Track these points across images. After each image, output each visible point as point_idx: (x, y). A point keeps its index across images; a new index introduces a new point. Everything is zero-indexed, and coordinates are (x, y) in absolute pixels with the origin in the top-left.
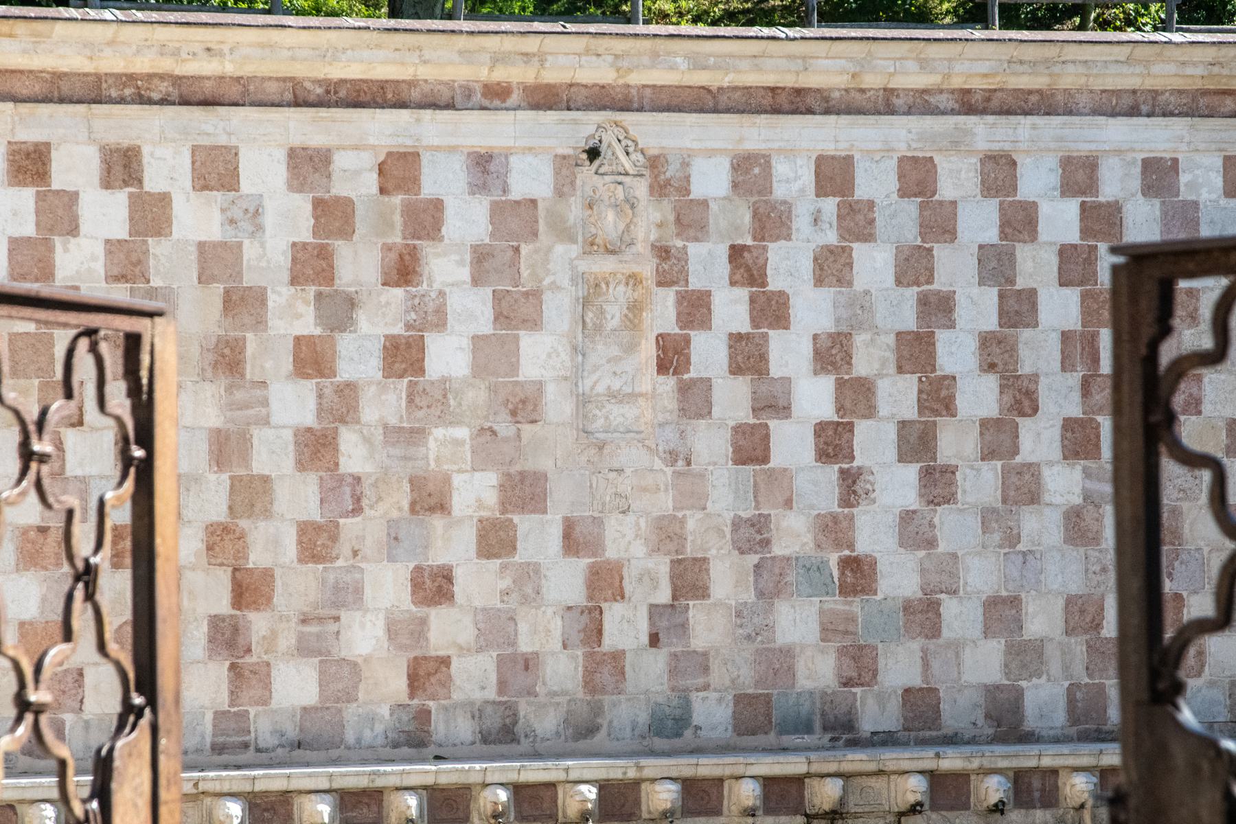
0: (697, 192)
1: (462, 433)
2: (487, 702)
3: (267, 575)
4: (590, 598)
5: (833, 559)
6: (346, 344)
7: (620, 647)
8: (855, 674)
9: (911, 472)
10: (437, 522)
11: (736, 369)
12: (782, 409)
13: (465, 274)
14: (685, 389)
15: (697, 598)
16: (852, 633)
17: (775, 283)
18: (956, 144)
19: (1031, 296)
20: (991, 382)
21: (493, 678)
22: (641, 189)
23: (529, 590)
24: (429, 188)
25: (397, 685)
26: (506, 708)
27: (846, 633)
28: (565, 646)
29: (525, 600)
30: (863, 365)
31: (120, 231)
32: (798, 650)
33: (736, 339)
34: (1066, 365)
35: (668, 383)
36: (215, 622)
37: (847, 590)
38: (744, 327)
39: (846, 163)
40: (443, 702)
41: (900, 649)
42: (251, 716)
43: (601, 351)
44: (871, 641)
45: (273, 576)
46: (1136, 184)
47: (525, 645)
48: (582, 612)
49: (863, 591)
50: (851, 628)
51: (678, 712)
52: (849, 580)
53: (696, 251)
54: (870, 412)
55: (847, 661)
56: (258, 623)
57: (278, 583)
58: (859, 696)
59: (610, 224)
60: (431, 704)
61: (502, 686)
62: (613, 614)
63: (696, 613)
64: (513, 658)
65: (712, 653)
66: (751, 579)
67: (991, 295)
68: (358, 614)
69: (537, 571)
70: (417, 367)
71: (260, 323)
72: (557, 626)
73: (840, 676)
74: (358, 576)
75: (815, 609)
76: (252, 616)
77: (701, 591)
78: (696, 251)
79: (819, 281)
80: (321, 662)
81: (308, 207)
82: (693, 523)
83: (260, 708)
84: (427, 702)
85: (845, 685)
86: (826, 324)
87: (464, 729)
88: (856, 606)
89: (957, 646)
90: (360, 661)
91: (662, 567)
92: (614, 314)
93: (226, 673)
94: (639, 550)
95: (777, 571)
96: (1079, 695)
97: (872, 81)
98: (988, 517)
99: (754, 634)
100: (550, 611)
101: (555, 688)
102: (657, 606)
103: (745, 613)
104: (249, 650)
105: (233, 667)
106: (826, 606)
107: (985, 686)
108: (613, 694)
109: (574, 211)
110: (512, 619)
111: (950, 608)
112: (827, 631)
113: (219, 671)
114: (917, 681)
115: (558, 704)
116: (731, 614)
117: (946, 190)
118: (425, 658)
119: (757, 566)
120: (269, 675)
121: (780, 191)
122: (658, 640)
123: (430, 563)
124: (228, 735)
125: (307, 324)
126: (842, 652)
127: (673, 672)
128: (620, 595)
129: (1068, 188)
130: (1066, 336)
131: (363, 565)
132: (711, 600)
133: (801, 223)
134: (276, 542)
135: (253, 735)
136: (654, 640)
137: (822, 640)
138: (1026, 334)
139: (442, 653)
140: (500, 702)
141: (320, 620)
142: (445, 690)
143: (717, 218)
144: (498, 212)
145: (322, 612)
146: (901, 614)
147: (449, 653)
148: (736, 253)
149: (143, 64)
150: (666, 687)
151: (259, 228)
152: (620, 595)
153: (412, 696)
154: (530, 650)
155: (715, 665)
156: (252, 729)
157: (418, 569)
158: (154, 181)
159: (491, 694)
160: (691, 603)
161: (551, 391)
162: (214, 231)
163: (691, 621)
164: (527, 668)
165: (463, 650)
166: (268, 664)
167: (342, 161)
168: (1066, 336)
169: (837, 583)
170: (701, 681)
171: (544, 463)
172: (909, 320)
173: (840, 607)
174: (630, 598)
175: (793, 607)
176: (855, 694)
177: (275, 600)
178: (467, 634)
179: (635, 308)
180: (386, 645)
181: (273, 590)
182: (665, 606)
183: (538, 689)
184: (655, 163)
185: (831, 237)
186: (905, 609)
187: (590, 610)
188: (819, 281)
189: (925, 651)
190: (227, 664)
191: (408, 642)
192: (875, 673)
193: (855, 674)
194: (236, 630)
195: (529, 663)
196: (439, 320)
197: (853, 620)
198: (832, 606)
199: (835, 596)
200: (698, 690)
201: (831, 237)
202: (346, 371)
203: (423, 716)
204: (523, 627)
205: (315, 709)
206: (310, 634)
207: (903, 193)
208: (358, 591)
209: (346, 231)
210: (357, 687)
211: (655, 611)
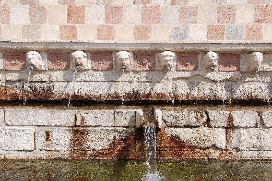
7: (158, 4)
8: (262, 18)
55: (259, 12)
58: (263, 27)
60: (76, 25)
65: (199, 8)
80: (30, 7)
83: (6, 25)
85: (258, 22)
90: (46, 7)
139: (81, 5)
155: (200, 13)
159: (102, 22)
166: (8, 7)
170: (193, 19)
183: (122, 21)
193: (262, 18)
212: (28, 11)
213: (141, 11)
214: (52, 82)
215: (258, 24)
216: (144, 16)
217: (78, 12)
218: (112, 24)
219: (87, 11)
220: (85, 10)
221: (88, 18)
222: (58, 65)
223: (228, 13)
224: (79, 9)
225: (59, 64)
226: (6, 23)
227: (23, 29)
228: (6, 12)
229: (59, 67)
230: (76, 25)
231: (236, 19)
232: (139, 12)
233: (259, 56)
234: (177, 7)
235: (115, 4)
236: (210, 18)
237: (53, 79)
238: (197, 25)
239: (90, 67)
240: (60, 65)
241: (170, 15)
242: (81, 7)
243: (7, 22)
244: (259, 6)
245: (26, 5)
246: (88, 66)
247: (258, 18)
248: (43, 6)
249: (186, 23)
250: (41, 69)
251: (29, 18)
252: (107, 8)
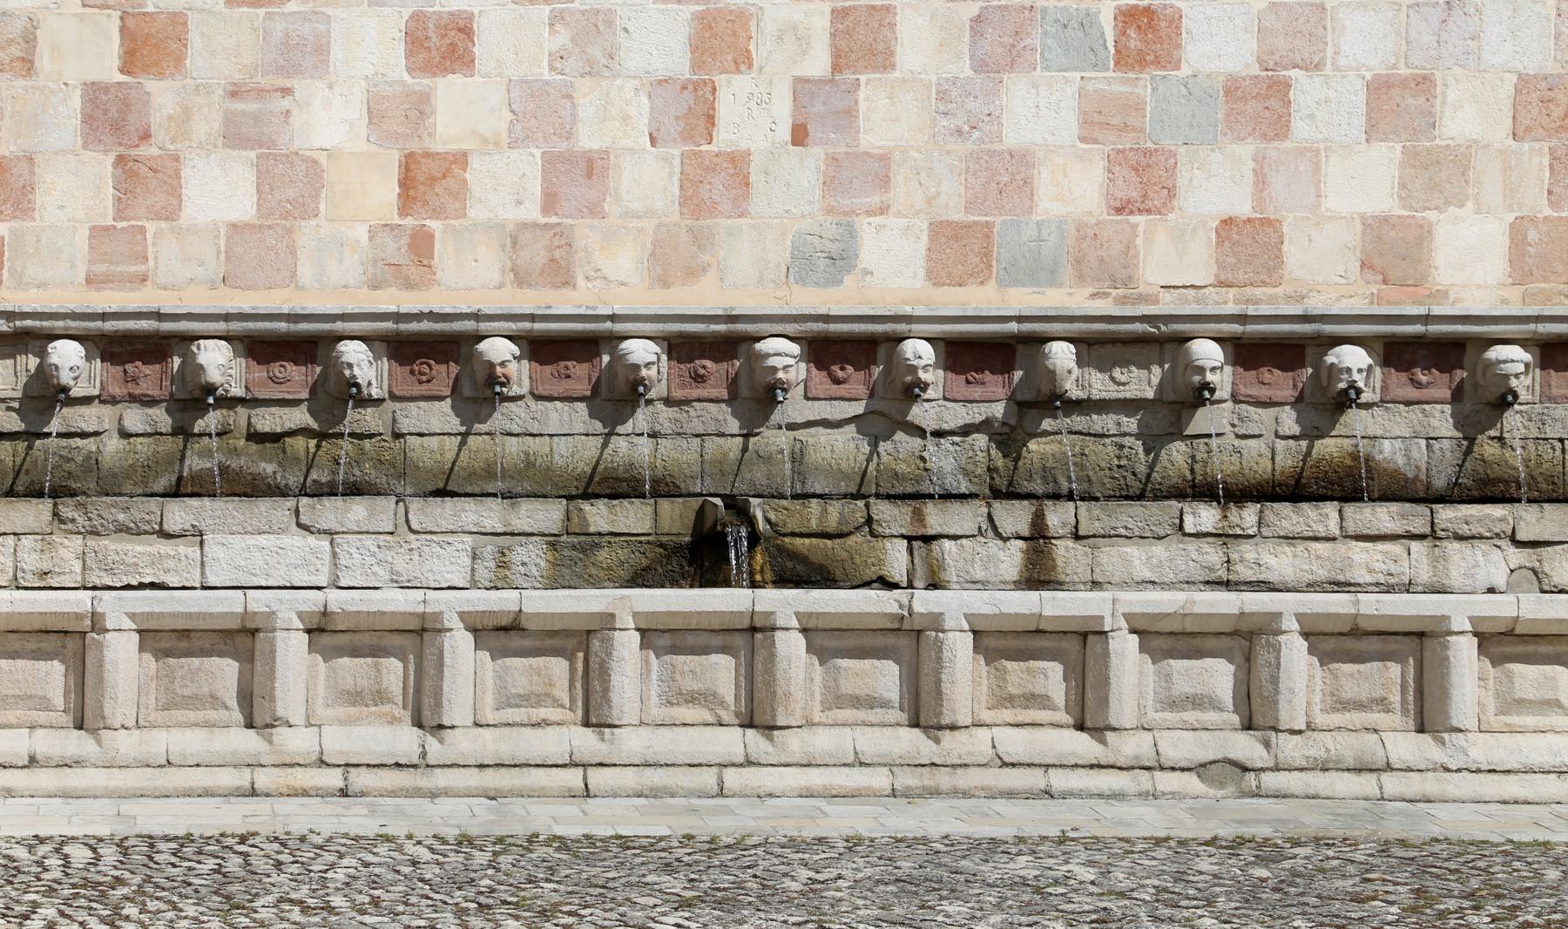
2: (524, 225)
4: (696, 66)
7: (744, 145)
8: (1135, 195)
15: (875, 69)
16: (1134, 129)
21: (536, 188)
23: (596, 52)
26: (555, 234)
27: (1125, 128)
28: (653, 141)
29: (590, 72)
32: (1040, 155)
36: (94, 93)
37: (1123, 59)
40: (453, 222)
41: (1216, 156)
42: (149, 236)
44: (1167, 143)
45: (185, 24)
47: (588, 140)
48: (684, 88)
49: (1157, 62)
50: (1131, 121)
51: (835, 248)
52: (1132, 44)
55: (1123, 173)
56: (162, 95)
57: (194, 37)
58: (1141, 229)
60: (434, 225)
61: (550, 202)
62: (733, 94)
63: (872, 94)
64: (568, 159)
65: (897, 156)
66: (967, 38)
68: (320, 84)
69: (610, 24)
72: (641, 110)
73: (1108, 195)
74: (322, 27)
75: (1072, 90)
76: (151, 85)
77: (882, 59)
83: (163, 224)
84: (427, 222)
88: (1143, 86)
89: (1313, 156)
90: (322, 158)
93: (110, 169)
95: (1011, 28)
96: (1532, 235)
99: (966, 128)
100: (630, 84)
101: (636, 206)
102: (807, 81)
103: (954, 94)
104: (146, 136)
105: (121, 160)
106: (1090, 86)
107: (1363, 219)
108: (730, 217)
110: (569, 96)
111: (1306, 90)
113: (101, 165)
115: (641, 230)
116: (929, 98)
118: (428, 155)
119: (977, 20)
120: (177, 175)
122: (807, 134)
123: (437, 8)
124: (111, 263)
126: (1116, 159)
127: (830, 184)
128: (743, 61)
131: (330, 11)
132: (897, 74)
135: (151, 263)
136: (799, 136)
137: (1083, 139)
139: (452, 147)
140: (545, 225)
141: (260, 93)
142: (458, 205)
145: (263, 81)
146: (1222, 99)
147: (466, 146)
150: (816, 207)
152: (743, 61)
153: (404, 211)
154: (595, 146)
155: (900, 178)
156: (150, 255)
157: (415, 17)
160: (863, 78)
163: (863, 106)
164: (590, 175)
165: (490, 144)
166: (177, 159)
169: (1112, 50)
170: (875, 200)
173: (1117, 88)
174: (761, 69)
175: (1035, 86)
176: (1135, 226)
177: (188, 62)
178: (498, 122)
180: (364, 133)
181: (185, 46)
182: (821, 82)
183: (607, 208)
186: (1227, 92)
187: (696, 86)
189: (1260, 161)
190: (111, 158)
191: (401, 129)
192: (1171, 193)
194: (126, 105)
195: (593, 167)
197: (1139, 108)
198: (1101, 86)
199: (1108, 70)
200: (869, 213)
204: (587, 109)
205: (250, 227)
206: (243, 113)
208: (321, 50)
210: (318, 195)
211: (802, 88)
212: (250, 175)
213: (678, 170)
214: (398, 436)
215: (1119, 218)
216: (692, 200)
217: (439, 175)
218: (570, 221)
219: (478, 173)
220: (469, 168)
221: (478, 195)
222: (420, 382)
223: (1006, 178)
224: (446, 165)
225: (424, 378)
226: (167, 219)
227: (228, 239)
228: (170, 176)
229: (424, 387)
230: (434, 225)
231: (1036, 197)
232: (671, 174)
233: (1062, 354)
234: (815, 155)
235: (581, 144)
236: (938, 194)
237: (405, 425)
238: (892, 222)
239: (524, 389)
240: (428, 381)
241: (788, 185)
242: (454, 155)
243: (170, 214)
244: (1122, 151)
245: (245, 153)
246: (520, 385)
247: (1119, 194)
248: (309, 153)
249: (846, 214)
250: (370, 395)
251: (255, 199)
252: (549, 160)
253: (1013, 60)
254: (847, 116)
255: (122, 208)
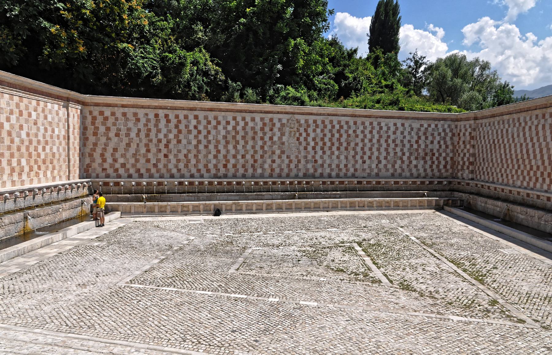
0: (301, 123)
1: (277, 146)
3: (257, 160)
5: (313, 160)
6: (265, 137)
9: (321, 151)
10: (274, 155)
11: (304, 141)
12: (309, 145)
13: (278, 130)
14: (299, 143)
17: (309, 132)
18: (327, 119)
19: (334, 134)
20: (330, 142)
22: (295, 122)
24: (274, 122)
25: (270, 171)
30: (317, 141)
31: (243, 125)
33: (305, 138)
34: (337, 141)
35: (297, 142)
36: (252, 164)
38: (305, 136)
39: (316, 120)
43: (291, 138)
46: (345, 123)
53: (301, 129)
54: (318, 145)
56: (256, 164)
59: (292, 126)
67: (330, 134)
70: (272, 139)
71: (257, 135)
77: (300, 163)
78: (301, 129)
79: (313, 132)
81: (180, 117)
82: (300, 156)
86: (314, 136)
87: (276, 176)
88: (316, 164)
89: (325, 169)
91: (296, 160)
92: (292, 135)
94: (294, 158)
97: (319, 112)
98: (329, 156)
109: (289, 124)
111: (325, 165)
112: (313, 166)
114: (321, 172)
117: (326, 123)
121: (309, 123)
125: (261, 135)
127: (297, 170)
128: (292, 163)
129: (338, 124)
130: (337, 138)
133: (311, 126)
134: (258, 157)
138: (333, 138)
143: (303, 126)
144: (281, 124)
148: (305, 129)
149: (246, 109)
151: (257, 125)
152: (292, 163)
158: (247, 120)
161: (286, 142)
162: (252, 125)
167: (266, 119)
168: (337, 138)
171: (285, 150)
172: (322, 136)
179: (295, 134)
184: (297, 120)
185: (314, 128)
188: (313, 132)
195: (283, 169)
196: (274, 134)
201: (314, 128)
202: (265, 140)
203: (272, 174)
207: (322, 123)
209: (266, 126)
211: (295, 164)
253: (308, 163)
254: (298, 166)
255: (253, 172)
